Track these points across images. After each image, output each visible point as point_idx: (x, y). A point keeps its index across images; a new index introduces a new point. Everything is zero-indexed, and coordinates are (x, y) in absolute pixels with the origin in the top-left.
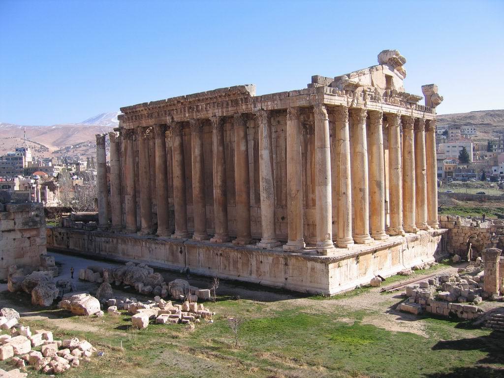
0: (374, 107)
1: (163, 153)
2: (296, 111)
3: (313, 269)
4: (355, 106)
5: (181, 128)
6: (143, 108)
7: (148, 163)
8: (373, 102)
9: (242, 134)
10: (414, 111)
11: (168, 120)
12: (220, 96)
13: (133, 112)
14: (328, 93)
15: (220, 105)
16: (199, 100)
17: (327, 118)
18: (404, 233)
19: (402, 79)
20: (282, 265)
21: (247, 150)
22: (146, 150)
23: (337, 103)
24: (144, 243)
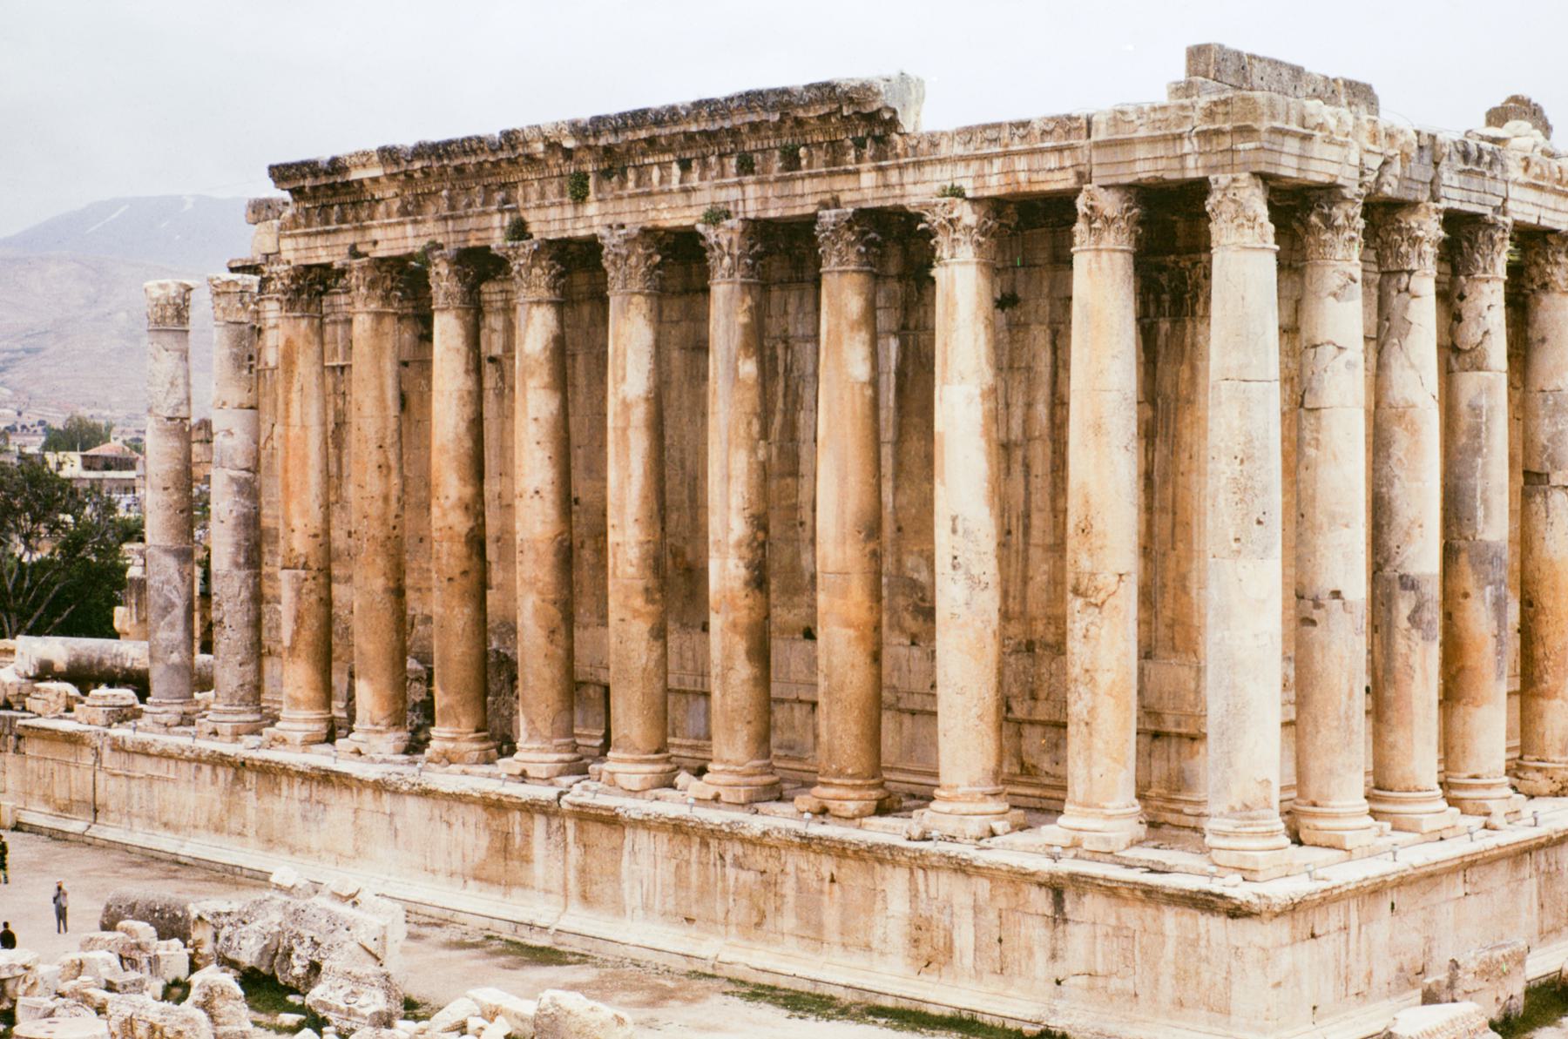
6: (378, 172)
9: (854, 304)
16: (651, 141)
21: (874, 383)
23: (1318, 173)
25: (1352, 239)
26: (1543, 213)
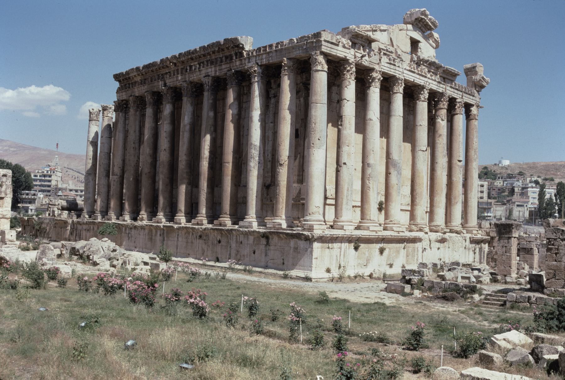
0: (393, 71)
1: (154, 125)
2: (292, 63)
3: (296, 249)
4: (366, 62)
5: (174, 94)
6: (135, 74)
7: (138, 138)
8: (390, 64)
10: (448, 88)
11: (160, 86)
12: (214, 52)
13: (126, 79)
14: (329, 39)
15: (212, 63)
16: (192, 59)
17: (326, 70)
18: (427, 230)
19: (433, 47)
20: (264, 246)
22: (137, 123)
24: (124, 228)
25: (352, 74)
26: (415, 79)
